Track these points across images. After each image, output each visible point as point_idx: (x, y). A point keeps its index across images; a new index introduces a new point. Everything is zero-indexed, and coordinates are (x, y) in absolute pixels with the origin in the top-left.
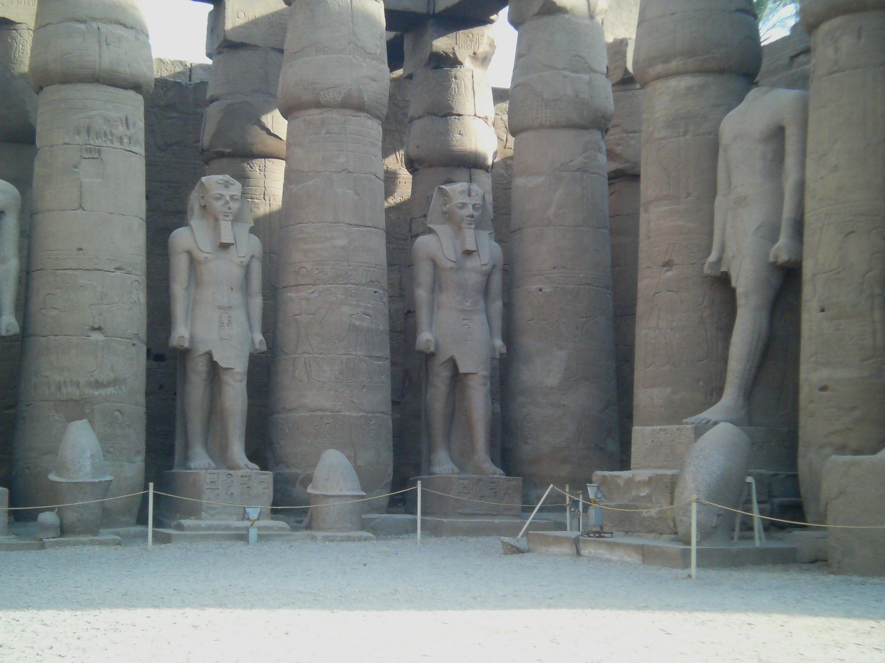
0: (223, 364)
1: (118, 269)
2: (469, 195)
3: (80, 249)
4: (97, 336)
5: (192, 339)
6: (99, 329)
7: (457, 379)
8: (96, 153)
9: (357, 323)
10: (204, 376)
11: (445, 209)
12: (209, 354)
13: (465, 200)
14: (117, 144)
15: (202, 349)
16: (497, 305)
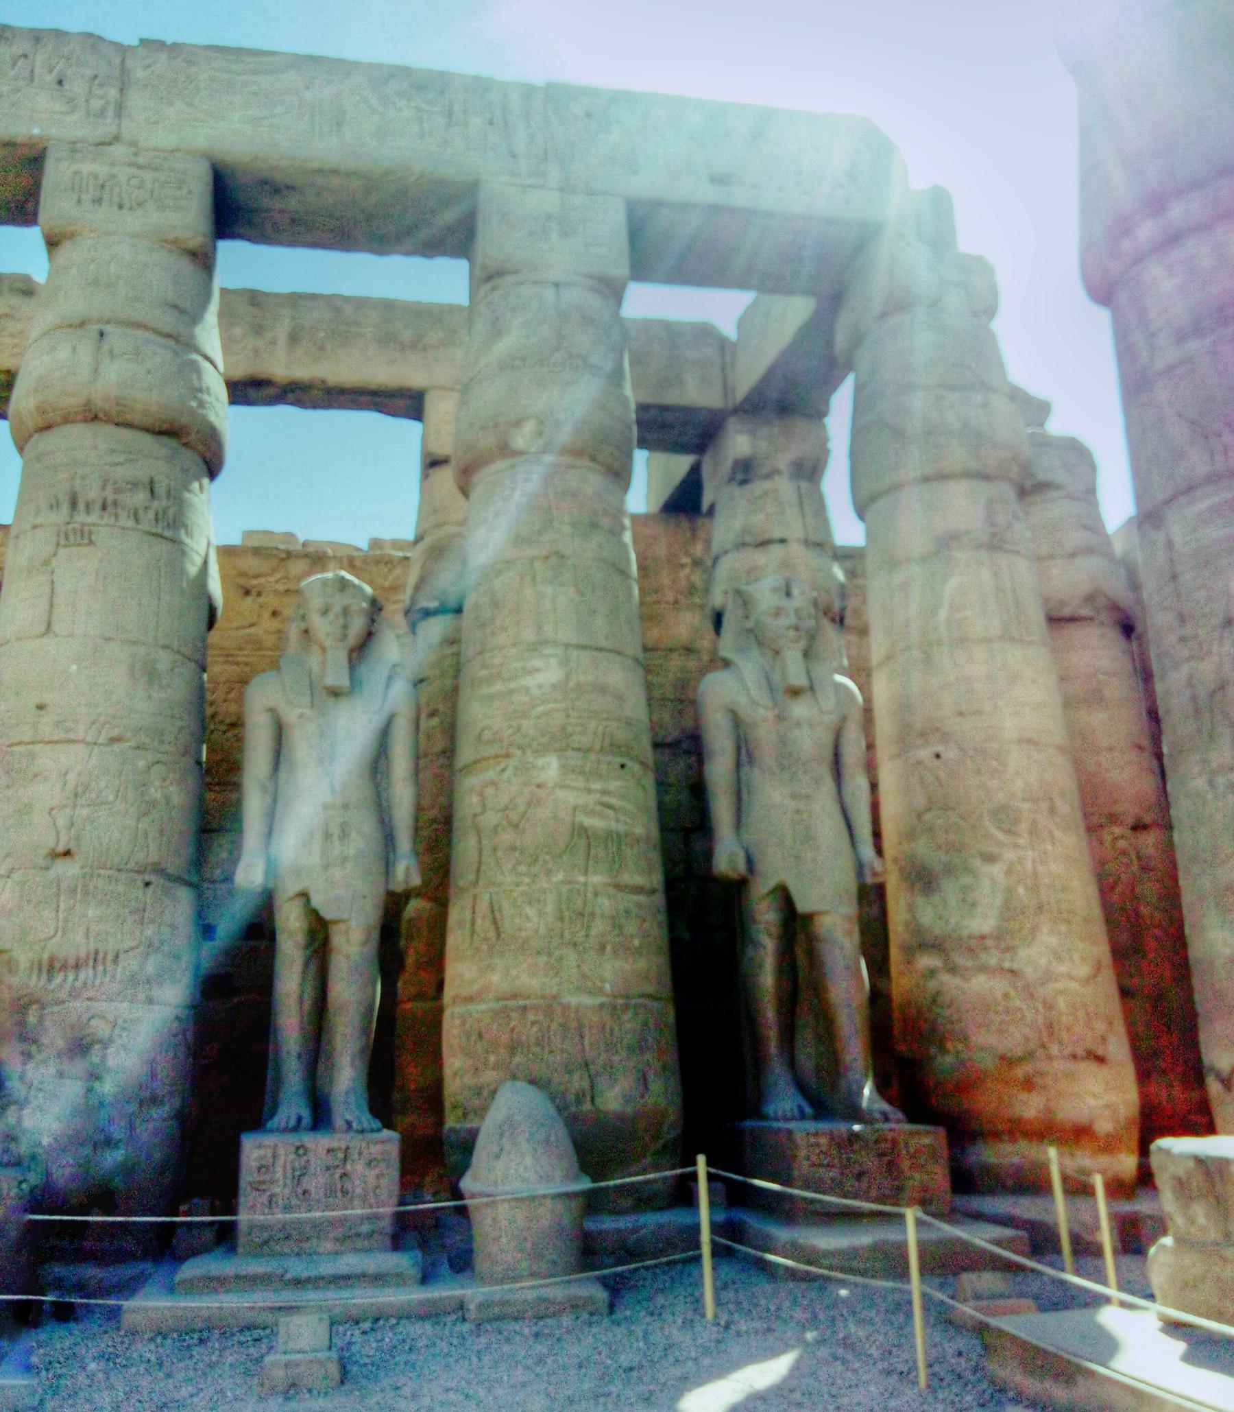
0: (327, 914)
1: (113, 740)
2: (788, 594)
3: (40, 707)
4: (68, 870)
5: (271, 868)
6: (67, 853)
7: (796, 925)
8: (85, 537)
9: (589, 822)
10: (301, 938)
11: (750, 624)
12: (304, 895)
13: (784, 602)
14: (131, 523)
15: (292, 888)
16: (857, 784)
